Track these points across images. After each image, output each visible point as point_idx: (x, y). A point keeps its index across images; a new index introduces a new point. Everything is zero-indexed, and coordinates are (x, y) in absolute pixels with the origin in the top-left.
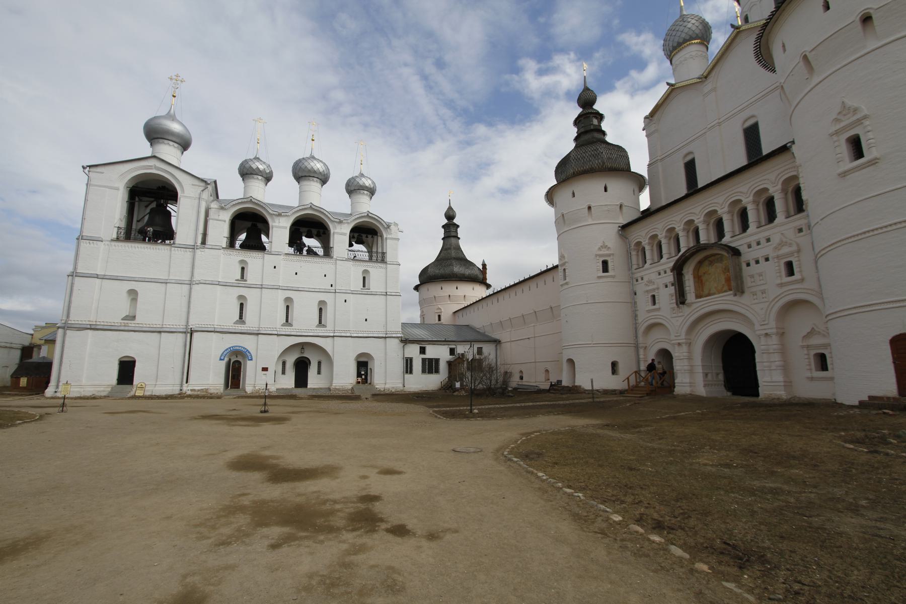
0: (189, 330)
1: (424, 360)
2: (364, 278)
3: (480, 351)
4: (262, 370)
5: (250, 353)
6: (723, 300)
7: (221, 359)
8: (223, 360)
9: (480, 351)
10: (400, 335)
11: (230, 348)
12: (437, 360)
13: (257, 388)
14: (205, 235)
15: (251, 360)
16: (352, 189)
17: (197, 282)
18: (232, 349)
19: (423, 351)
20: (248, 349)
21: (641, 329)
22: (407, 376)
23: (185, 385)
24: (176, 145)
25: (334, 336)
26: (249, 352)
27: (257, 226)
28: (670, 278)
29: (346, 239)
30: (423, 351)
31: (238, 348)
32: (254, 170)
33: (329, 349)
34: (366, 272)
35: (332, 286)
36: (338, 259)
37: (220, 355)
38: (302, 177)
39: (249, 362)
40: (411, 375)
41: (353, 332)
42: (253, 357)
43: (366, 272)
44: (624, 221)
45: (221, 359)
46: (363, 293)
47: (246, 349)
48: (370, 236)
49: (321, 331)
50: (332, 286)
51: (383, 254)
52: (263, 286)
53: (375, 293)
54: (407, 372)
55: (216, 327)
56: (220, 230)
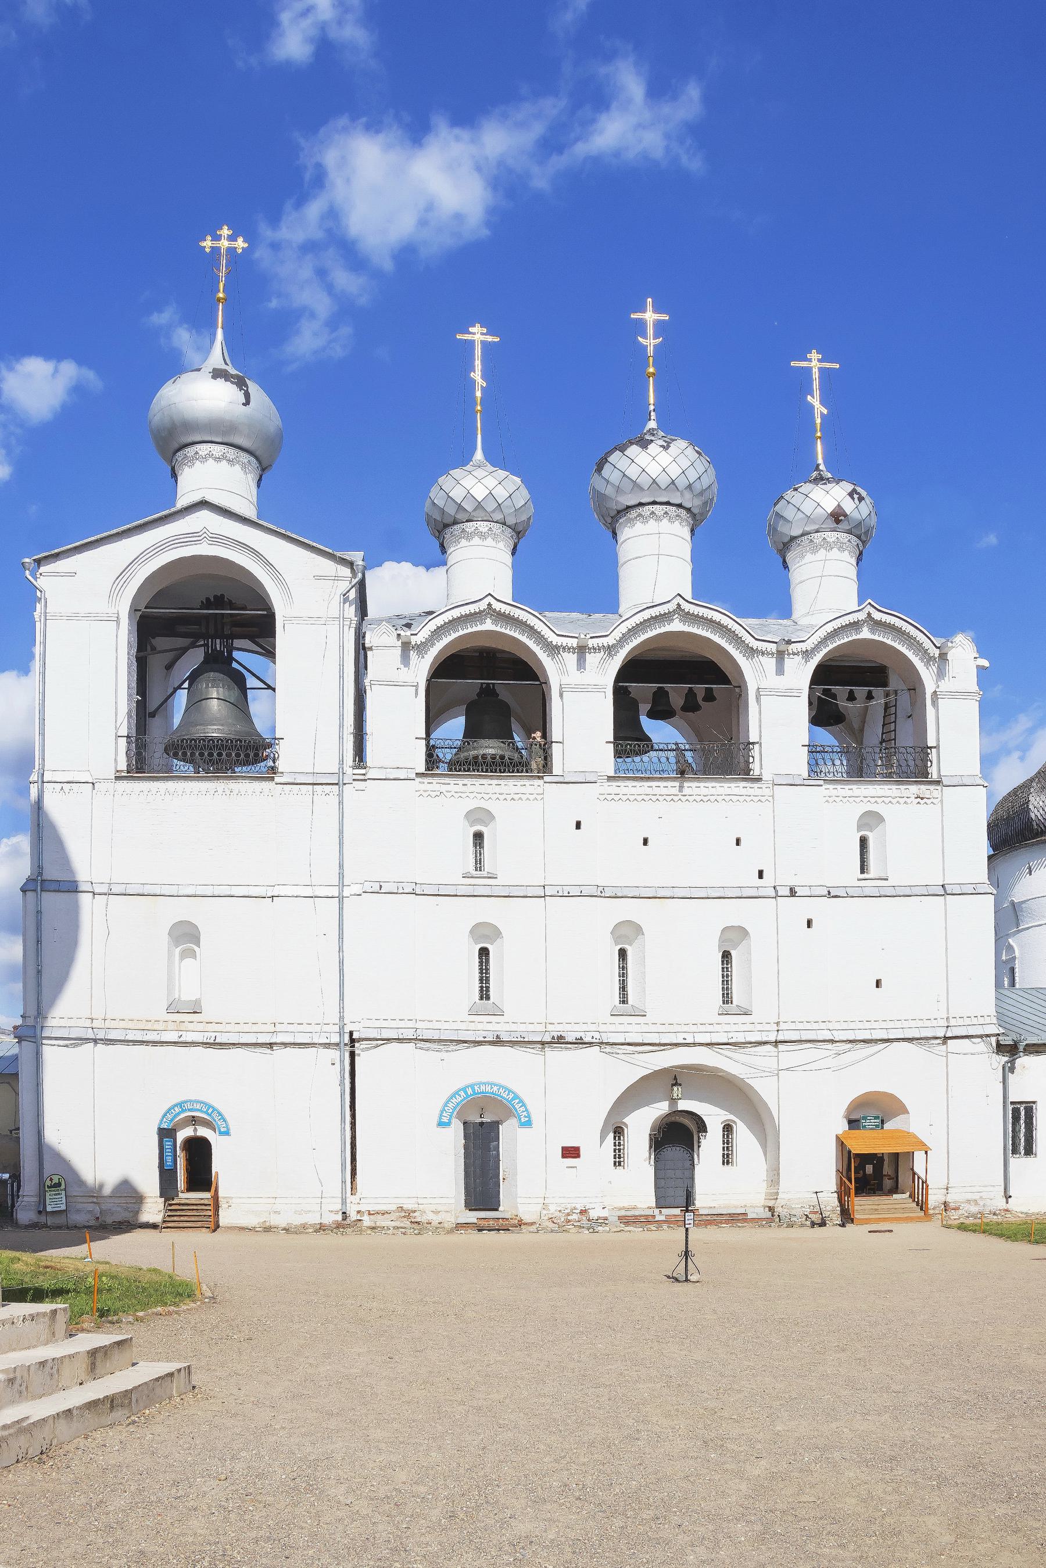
0: (347, 1039)
2: (863, 842)
4: (564, 1156)
5: (524, 1105)
7: (441, 1124)
8: (448, 1124)
10: (994, 1030)
11: (464, 1089)
13: (553, 1208)
15: (528, 1124)
16: (794, 533)
17: (357, 889)
18: (470, 1091)
20: (520, 1094)
22: (1017, 1163)
23: (350, 1198)
24: (245, 457)
25: (776, 1043)
26: (521, 1101)
27: (498, 695)
29: (800, 709)
31: (488, 1089)
32: (479, 506)
33: (764, 1088)
34: (871, 819)
35: (761, 874)
36: (778, 781)
37: (438, 1112)
38: (629, 508)
39: (522, 1132)
40: (1030, 1160)
41: (837, 1026)
42: (534, 1118)
43: (871, 819)
45: (441, 1124)
46: (867, 892)
47: (510, 1091)
49: (734, 1028)
50: (761, 874)
51: (923, 751)
52: (549, 891)
53: (908, 892)
54: (1015, 1151)
55: (420, 1025)
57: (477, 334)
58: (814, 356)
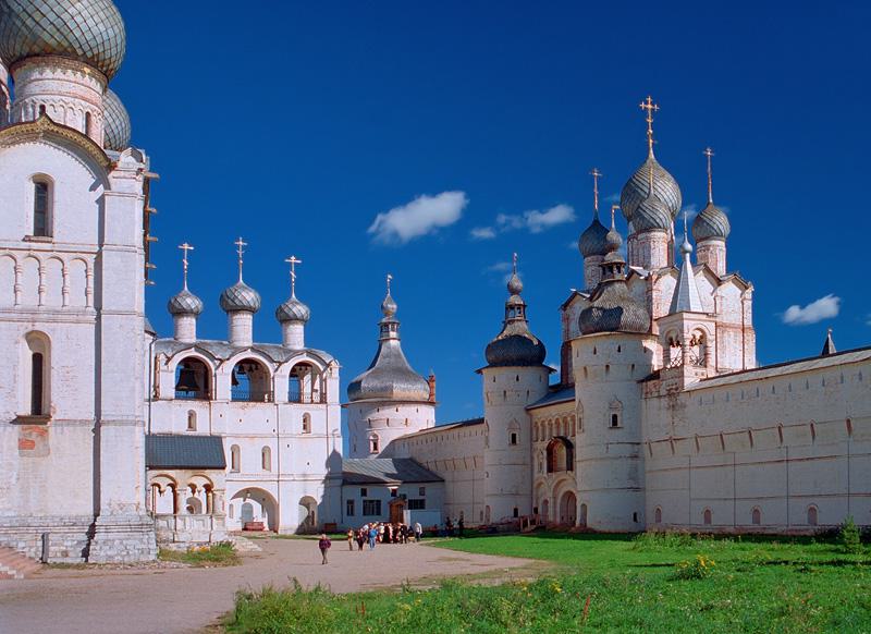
1: (364, 501)
3: (422, 493)
6: (562, 475)
9: (422, 493)
12: (379, 502)
14: (156, 387)
19: (364, 493)
21: (535, 485)
28: (545, 453)
30: (364, 493)
44: (531, 401)
48: (303, 368)
56: (168, 381)
57: (186, 246)
58: (293, 258)
